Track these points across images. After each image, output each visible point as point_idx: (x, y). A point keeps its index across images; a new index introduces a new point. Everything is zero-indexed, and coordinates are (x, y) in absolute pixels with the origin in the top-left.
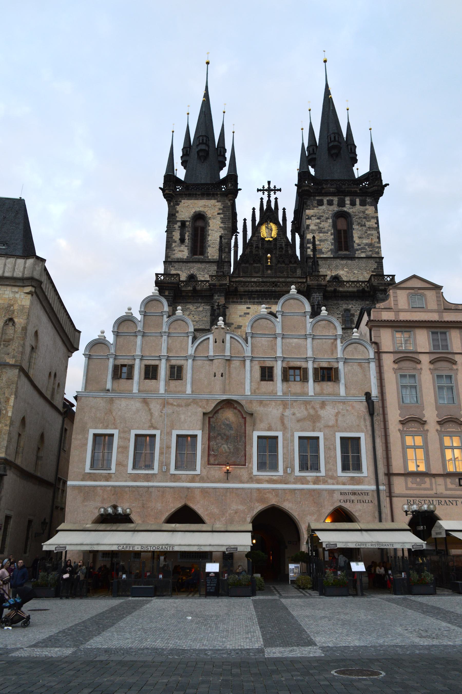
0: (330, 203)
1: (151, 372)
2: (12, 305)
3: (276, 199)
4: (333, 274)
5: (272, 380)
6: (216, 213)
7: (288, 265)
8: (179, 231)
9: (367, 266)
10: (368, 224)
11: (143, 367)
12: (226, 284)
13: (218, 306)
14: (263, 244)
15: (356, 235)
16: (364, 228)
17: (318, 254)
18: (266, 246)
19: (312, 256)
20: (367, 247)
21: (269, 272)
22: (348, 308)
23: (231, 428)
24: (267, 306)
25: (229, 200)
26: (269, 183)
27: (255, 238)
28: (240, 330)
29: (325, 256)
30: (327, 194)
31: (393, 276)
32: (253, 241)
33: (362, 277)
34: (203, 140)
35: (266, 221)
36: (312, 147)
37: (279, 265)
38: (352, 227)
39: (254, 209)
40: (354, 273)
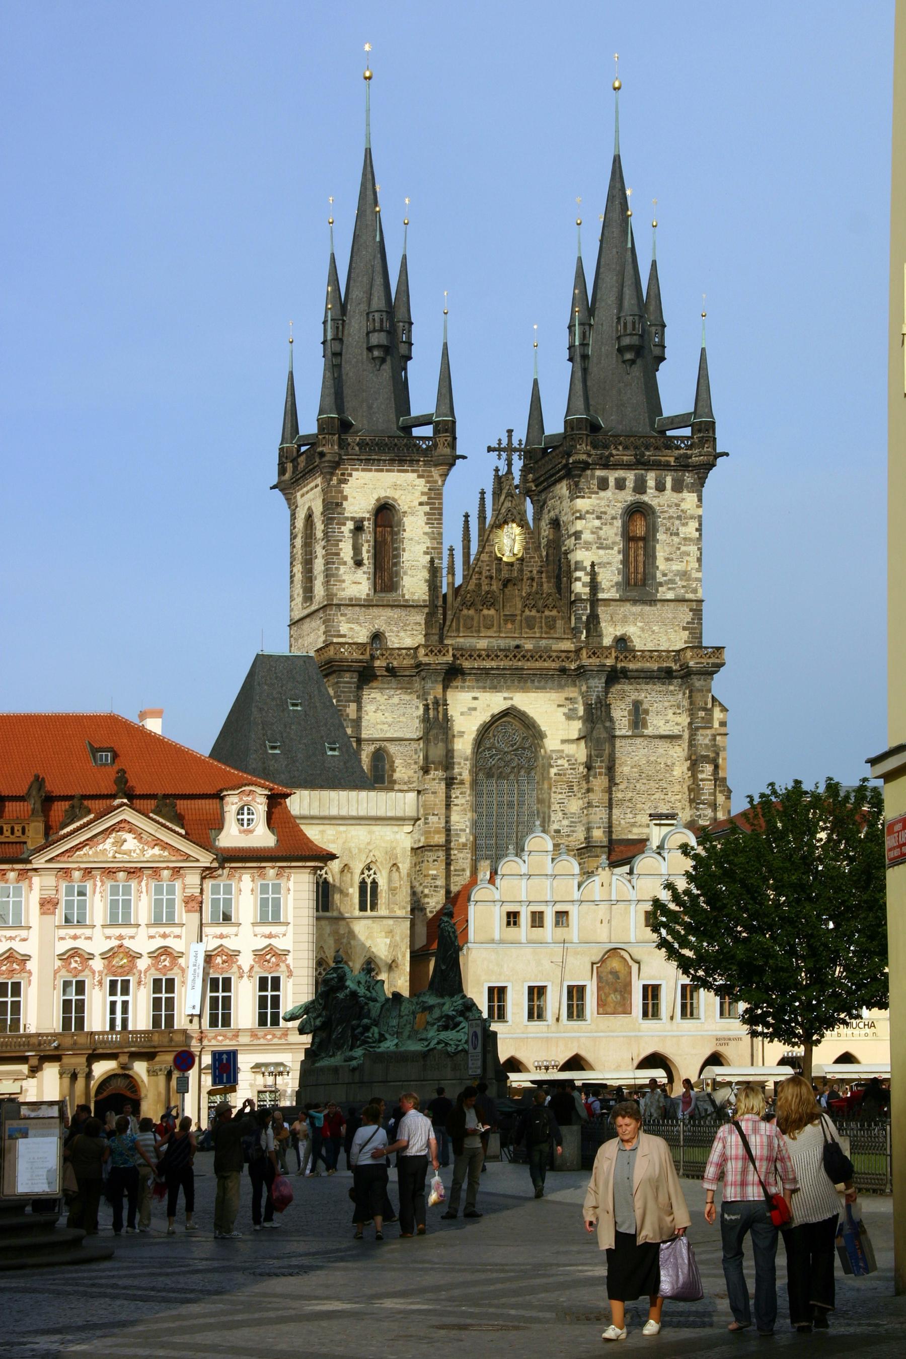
1: (537, 919)
2: (395, 848)
4: (618, 634)
6: (416, 503)
7: (543, 612)
11: (529, 915)
14: (499, 570)
18: (505, 574)
19: (584, 597)
22: (640, 698)
23: (618, 978)
25: (441, 475)
27: (484, 557)
31: (719, 649)
32: (482, 561)
35: (506, 522)
37: (527, 613)
39: (483, 493)
40: (653, 632)
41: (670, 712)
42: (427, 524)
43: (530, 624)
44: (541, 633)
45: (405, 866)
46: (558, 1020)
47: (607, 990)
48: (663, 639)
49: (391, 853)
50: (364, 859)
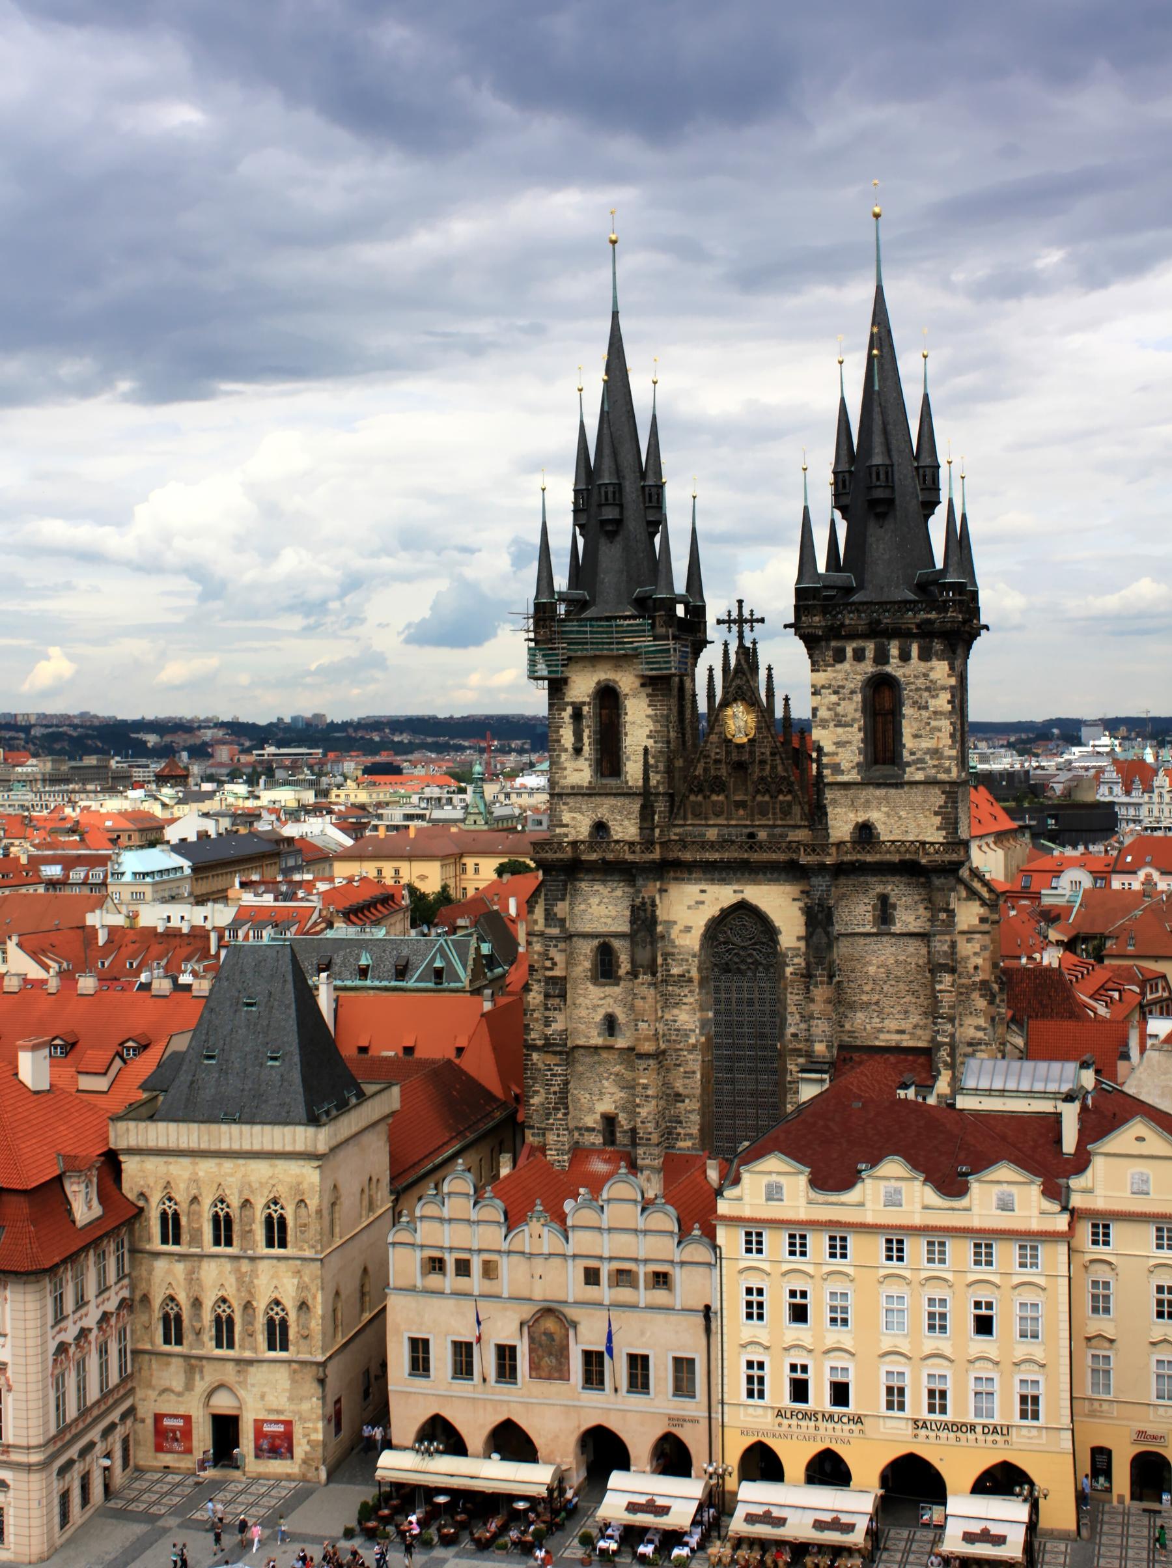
0: (859, 656)
1: (463, 1268)
3: (754, 643)
4: (860, 820)
5: (597, 1283)
8: (571, 727)
9: (924, 801)
10: (933, 704)
12: (653, 862)
13: (643, 904)
14: (728, 753)
15: (907, 730)
16: (925, 714)
17: (833, 774)
18: (735, 757)
20: (928, 757)
21: (741, 812)
23: (553, 1340)
24: (736, 887)
26: (740, 602)
27: (714, 738)
28: (689, 935)
29: (845, 778)
30: (851, 637)
33: (914, 825)
34: (606, 493)
35: (735, 700)
36: (841, 476)
37: (759, 798)
38: (901, 710)
39: (711, 670)
40: (900, 818)
41: (921, 907)
42: (649, 706)
43: (763, 811)
44: (775, 819)
45: (313, 1203)
46: (484, 1380)
47: (540, 1352)
48: (912, 825)
49: (297, 1188)
50: (266, 1194)
